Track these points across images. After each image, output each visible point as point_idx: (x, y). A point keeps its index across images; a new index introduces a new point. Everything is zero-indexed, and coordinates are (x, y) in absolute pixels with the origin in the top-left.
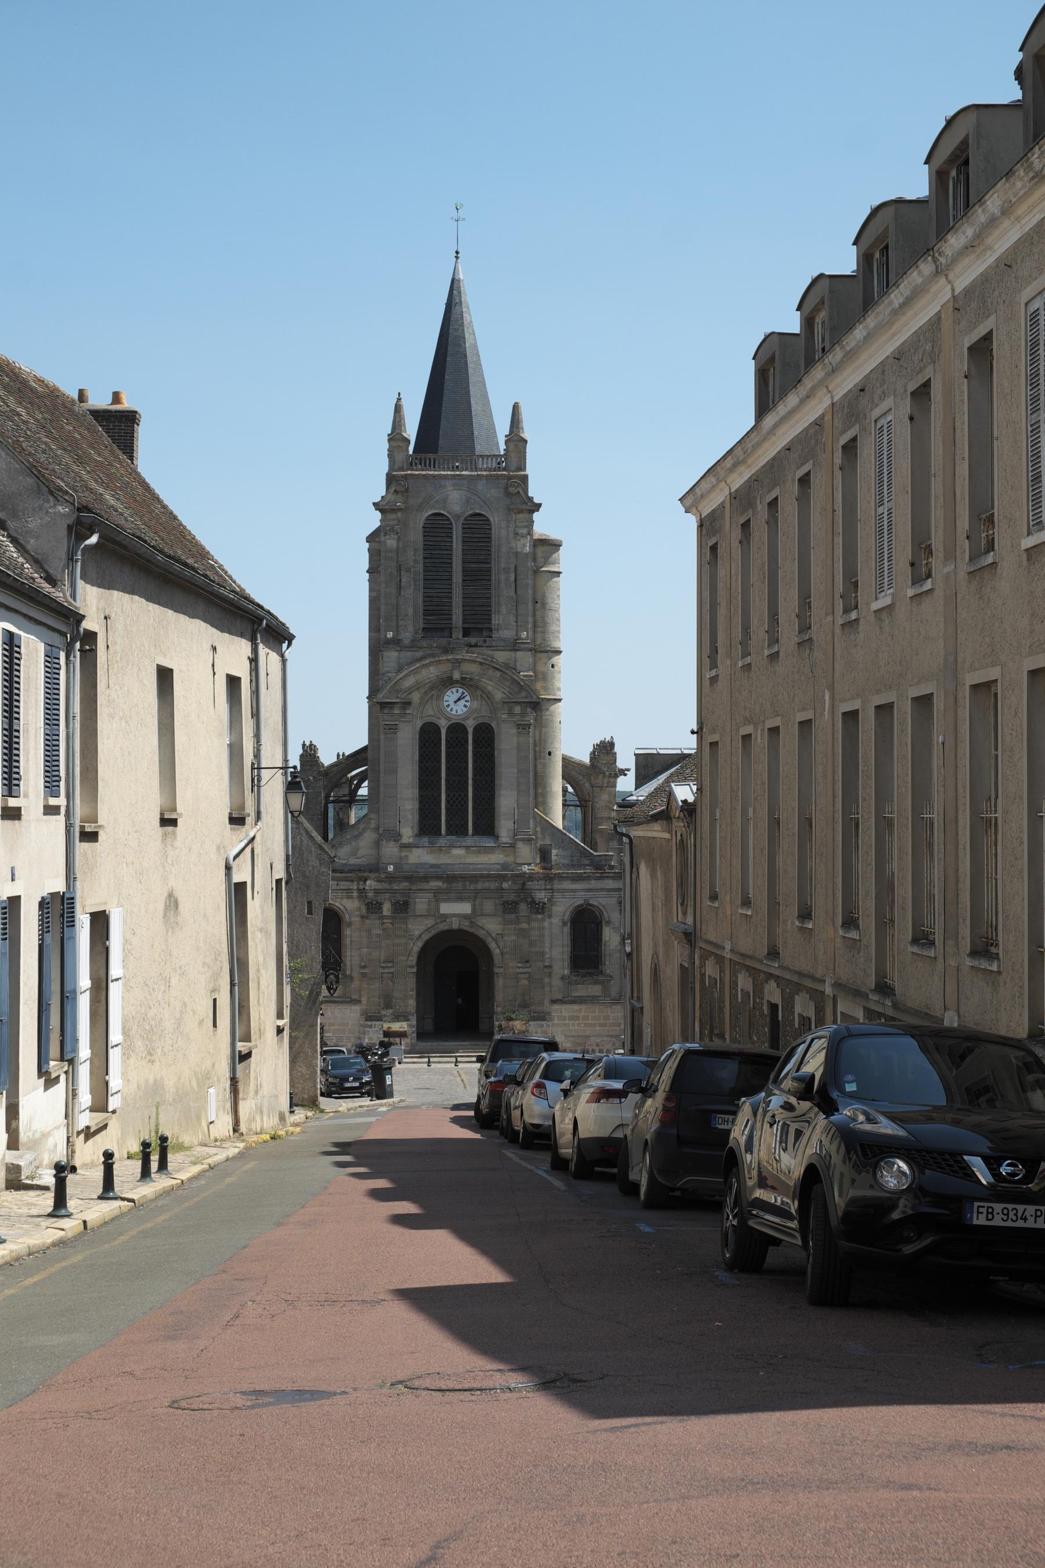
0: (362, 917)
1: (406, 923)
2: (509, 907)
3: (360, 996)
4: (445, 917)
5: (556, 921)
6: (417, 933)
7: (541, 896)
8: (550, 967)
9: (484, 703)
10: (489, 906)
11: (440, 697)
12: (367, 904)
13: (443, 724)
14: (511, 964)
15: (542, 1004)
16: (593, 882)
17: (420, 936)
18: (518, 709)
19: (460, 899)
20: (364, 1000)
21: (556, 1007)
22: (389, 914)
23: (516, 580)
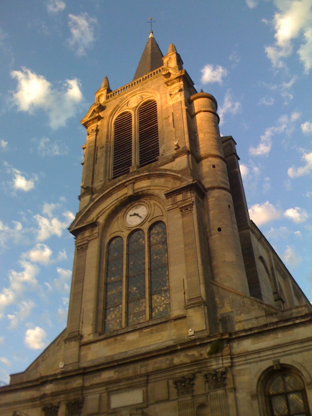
5: (243, 396)
9: (156, 207)
10: (160, 388)
11: (124, 216)
13: (125, 234)
16: (280, 335)
18: (179, 198)
19: (131, 387)
23: (173, 120)
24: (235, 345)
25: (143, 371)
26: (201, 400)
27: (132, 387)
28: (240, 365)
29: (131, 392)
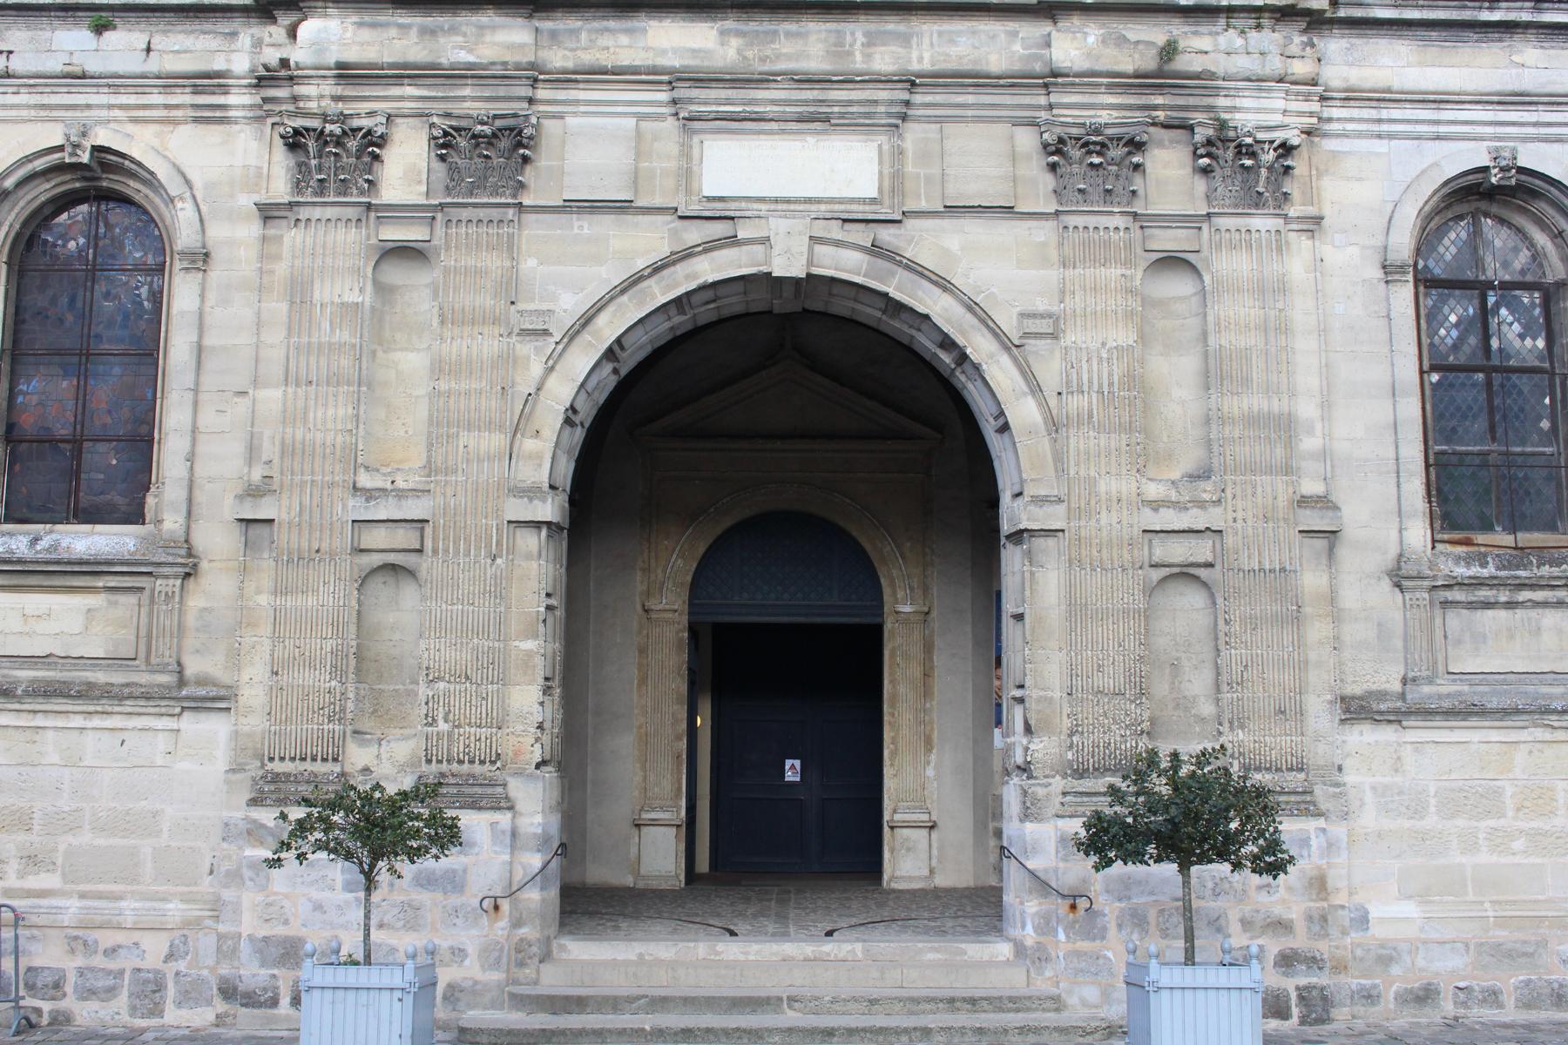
0: (268, 213)
1: (510, 248)
2: (1092, 162)
3: (235, 658)
4: (723, 216)
6: (570, 305)
7: (1258, 114)
8: (1324, 502)
12: (294, 142)
14: (1108, 486)
15: (1289, 713)
17: (587, 320)
19: (817, 120)
20: (254, 687)
21: (1364, 736)
22: (414, 195)
24: (1335, 45)
25: (884, 60)
26: (1169, 240)
27: (826, 119)
28: (1344, 135)
29: (811, 139)
